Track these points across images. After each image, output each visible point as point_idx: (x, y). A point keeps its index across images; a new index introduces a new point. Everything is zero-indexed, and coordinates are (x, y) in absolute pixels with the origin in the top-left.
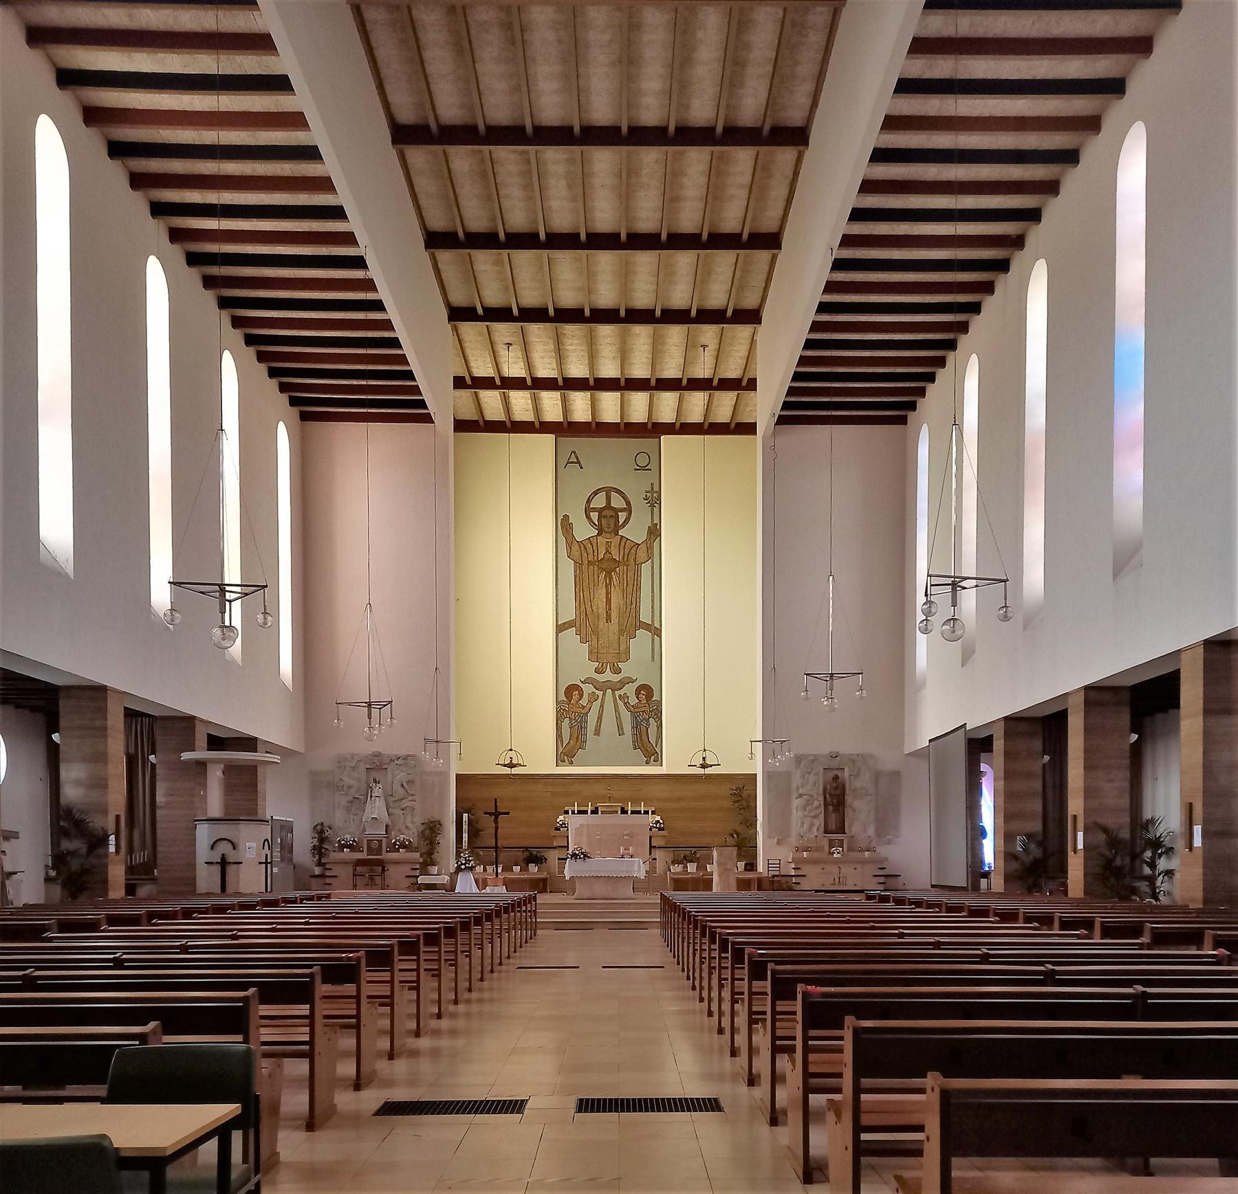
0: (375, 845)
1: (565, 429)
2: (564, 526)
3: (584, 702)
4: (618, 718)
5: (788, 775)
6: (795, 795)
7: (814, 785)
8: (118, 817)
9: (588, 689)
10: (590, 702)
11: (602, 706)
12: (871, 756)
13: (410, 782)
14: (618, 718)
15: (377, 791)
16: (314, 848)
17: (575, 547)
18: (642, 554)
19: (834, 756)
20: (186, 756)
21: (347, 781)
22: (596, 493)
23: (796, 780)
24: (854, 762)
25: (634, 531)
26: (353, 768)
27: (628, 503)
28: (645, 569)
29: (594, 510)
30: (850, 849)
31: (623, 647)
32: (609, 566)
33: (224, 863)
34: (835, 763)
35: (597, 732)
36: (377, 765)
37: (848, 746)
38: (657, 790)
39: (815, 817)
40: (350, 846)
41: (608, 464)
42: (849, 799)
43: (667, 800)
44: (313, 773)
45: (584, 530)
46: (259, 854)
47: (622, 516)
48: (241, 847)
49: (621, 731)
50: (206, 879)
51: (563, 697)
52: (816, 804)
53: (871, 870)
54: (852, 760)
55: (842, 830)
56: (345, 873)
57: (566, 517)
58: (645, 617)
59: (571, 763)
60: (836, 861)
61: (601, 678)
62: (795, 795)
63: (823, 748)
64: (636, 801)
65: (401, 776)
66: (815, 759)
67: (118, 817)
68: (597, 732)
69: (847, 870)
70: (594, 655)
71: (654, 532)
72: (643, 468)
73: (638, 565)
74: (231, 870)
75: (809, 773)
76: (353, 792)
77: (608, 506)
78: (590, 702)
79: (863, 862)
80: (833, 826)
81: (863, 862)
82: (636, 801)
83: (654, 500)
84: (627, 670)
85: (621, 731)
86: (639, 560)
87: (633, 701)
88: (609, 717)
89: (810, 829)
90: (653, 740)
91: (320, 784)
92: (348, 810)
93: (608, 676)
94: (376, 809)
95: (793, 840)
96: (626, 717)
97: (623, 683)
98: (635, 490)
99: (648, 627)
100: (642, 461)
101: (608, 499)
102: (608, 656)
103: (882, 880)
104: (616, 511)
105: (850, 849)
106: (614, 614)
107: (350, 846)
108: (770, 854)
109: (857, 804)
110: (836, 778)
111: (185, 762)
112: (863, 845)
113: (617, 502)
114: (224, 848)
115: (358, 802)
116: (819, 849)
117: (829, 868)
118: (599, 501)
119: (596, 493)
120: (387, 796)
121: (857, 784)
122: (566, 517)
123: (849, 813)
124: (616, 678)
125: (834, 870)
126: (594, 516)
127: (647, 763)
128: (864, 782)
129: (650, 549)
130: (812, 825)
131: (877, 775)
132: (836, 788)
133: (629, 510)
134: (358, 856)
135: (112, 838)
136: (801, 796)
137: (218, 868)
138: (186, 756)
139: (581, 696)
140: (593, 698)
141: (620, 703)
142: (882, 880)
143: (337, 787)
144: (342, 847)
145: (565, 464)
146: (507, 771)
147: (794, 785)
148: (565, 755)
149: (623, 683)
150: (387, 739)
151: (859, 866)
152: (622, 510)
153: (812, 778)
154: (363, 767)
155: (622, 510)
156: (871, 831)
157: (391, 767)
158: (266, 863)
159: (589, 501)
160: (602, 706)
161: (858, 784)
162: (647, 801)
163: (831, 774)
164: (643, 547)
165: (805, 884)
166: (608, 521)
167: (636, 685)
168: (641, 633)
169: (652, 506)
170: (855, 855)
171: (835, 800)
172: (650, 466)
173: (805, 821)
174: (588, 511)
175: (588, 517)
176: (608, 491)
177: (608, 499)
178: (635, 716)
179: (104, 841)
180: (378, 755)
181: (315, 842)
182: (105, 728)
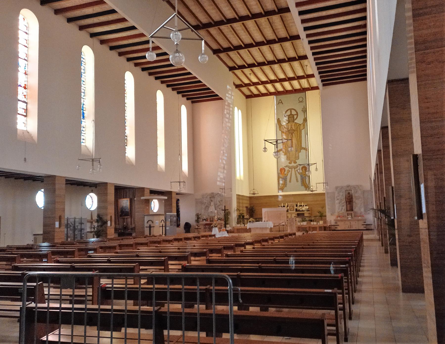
1: (277, 93)
2: (279, 121)
3: (286, 172)
4: (296, 177)
5: (334, 193)
6: (336, 199)
7: (342, 196)
8: (111, 217)
9: (287, 169)
11: (291, 174)
12: (361, 186)
13: (221, 201)
14: (296, 177)
15: (212, 204)
16: (196, 220)
18: (302, 127)
19: (348, 186)
20: (142, 198)
21: (205, 201)
22: (287, 111)
23: (336, 194)
24: (355, 188)
25: (299, 121)
26: (206, 197)
27: (297, 113)
28: (303, 132)
30: (355, 216)
31: (297, 155)
33: (150, 227)
34: (348, 189)
35: (290, 181)
36: (212, 196)
37: (353, 183)
38: (309, 199)
39: (343, 206)
40: (205, 220)
41: (291, 101)
42: (354, 200)
43: (312, 201)
44: (196, 199)
46: (159, 224)
47: (295, 117)
50: (147, 232)
51: (279, 172)
52: (343, 202)
53: (362, 223)
54: (354, 187)
55: (352, 210)
56: (202, 227)
58: (303, 146)
60: (349, 220)
61: (291, 165)
62: (336, 199)
63: (345, 184)
64: (301, 202)
65: (219, 199)
66: (342, 187)
67: (111, 217)
68: (290, 181)
69: (353, 223)
70: (288, 158)
71: (305, 120)
72: (301, 102)
74: (152, 228)
75: (340, 192)
76: (206, 204)
77: (291, 114)
79: (358, 220)
80: (348, 209)
81: (358, 220)
83: (305, 111)
84: (299, 162)
87: (301, 171)
89: (341, 210)
90: (307, 183)
91: (198, 202)
92: (205, 209)
93: (293, 164)
94: (212, 209)
95: (336, 214)
96: (299, 176)
97: (297, 166)
100: (301, 100)
101: (291, 112)
102: (292, 158)
103: (365, 226)
104: (293, 115)
106: (294, 146)
107: (205, 220)
108: (331, 219)
109: (357, 201)
110: (349, 193)
111: (143, 200)
113: (294, 113)
114: (150, 223)
115: (207, 207)
117: (347, 222)
118: (289, 113)
119: (287, 111)
120: (215, 205)
121: (355, 195)
123: (354, 204)
124: (295, 165)
125: (348, 223)
127: (306, 190)
129: (304, 125)
130: (342, 209)
131: (364, 192)
132: (349, 197)
134: (207, 222)
135: (109, 223)
136: (338, 199)
137: (148, 229)
138: (142, 198)
139: (285, 171)
141: (297, 172)
142: (365, 226)
143: (202, 203)
145: (279, 103)
146: (253, 195)
147: (336, 196)
148: (281, 189)
149: (297, 166)
151: (357, 222)
152: (295, 115)
153: (341, 194)
154: (209, 197)
155: (295, 115)
156: (362, 210)
157: (216, 196)
158: (163, 226)
160: (291, 174)
161: (357, 195)
162: (304, 202)
163: (347, 192)
164: (302, 125)
165: (339, 228)
166: (291, 118)
169: (304, 113)
170: (356, 218)
171: (349, 200)
172: (303, 101)
176: (291, 110)
177: (291, 112)
178: (301, 176)
179: (106, 223)
180: (213, 193)
181: (197, 219)
182: (107, 193)
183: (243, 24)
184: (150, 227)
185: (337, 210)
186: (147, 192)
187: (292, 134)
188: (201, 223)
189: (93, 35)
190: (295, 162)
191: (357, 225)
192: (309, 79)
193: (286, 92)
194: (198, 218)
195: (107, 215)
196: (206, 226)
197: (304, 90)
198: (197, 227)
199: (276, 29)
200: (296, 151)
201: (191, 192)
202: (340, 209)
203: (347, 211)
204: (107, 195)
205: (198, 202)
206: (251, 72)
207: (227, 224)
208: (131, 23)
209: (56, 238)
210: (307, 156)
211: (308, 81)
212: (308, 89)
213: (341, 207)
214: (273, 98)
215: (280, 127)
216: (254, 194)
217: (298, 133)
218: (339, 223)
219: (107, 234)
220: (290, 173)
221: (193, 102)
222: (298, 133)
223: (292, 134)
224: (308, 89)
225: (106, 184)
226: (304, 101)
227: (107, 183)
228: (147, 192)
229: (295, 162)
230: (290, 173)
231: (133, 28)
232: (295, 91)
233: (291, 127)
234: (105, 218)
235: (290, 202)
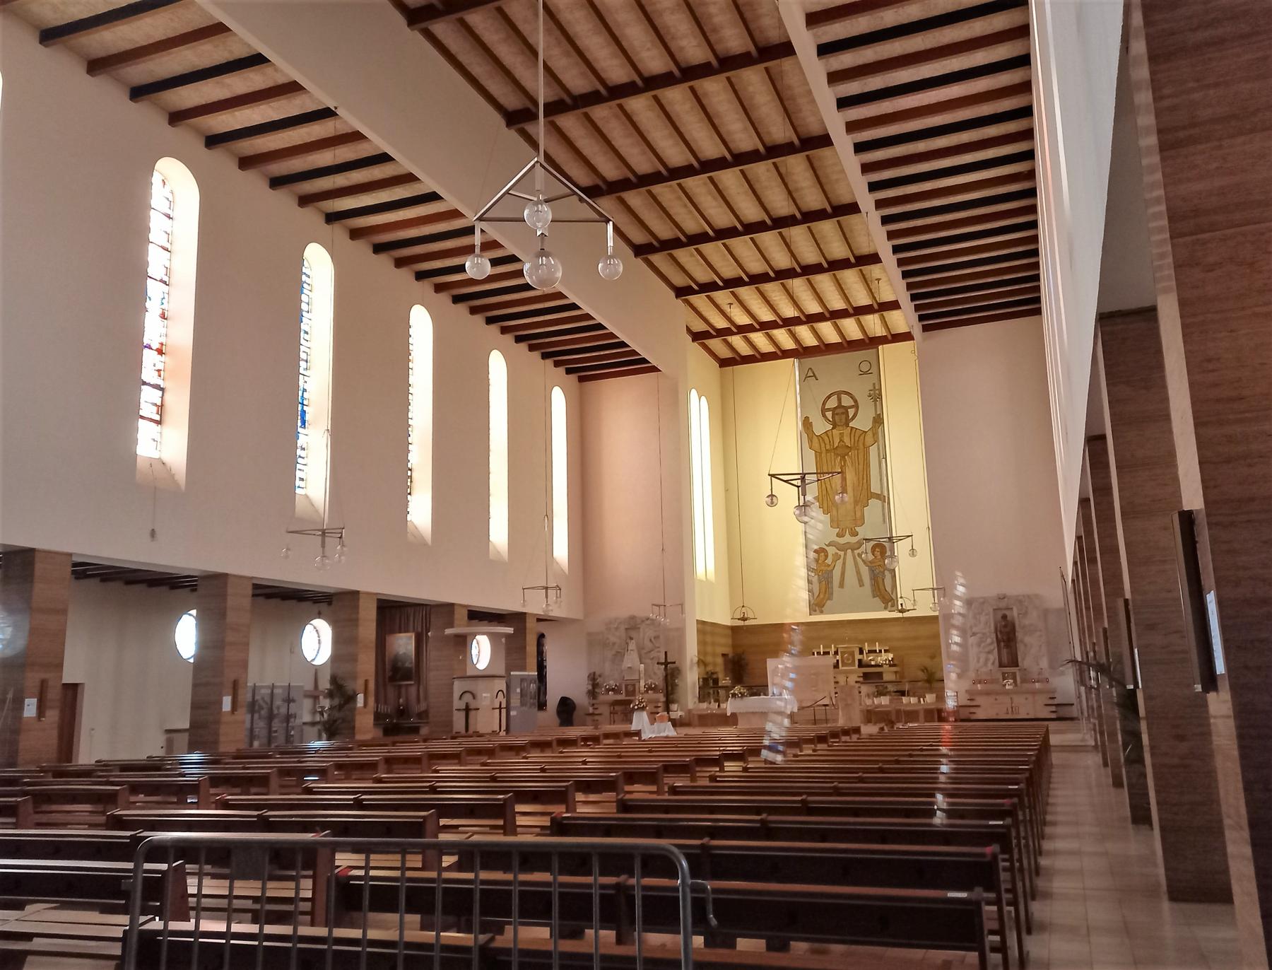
0: (630, 688)
1: (801, 352)
2: (807, 424)
3: (829, 561)
4: (858, 573)
7: (986, 625)
8: (366, 681)
9: (831, 551)
10: (835, 561)
11: (844, 563)
12: (1037, 596)
13: (657, 637)
14: (858, 573)
15: (632, 645)
16: (589, 692)
17: (815, 440)
18: (869, 438)
20: (448, 631)
21: (613, 639)
22: (829, 397)
24: (1020, 602)
25: (862, 422)
26: (617, 629)
27: (856, 401)
28: (873, 451)
29: (829, 410)
30: (1024, 681)
31: (858, 514)
32: (842, 453)
33: (467, 710)
34: (1003, 604)
35: (842, 585)
36: (633, 625)
37: (1015, 588)
38: (895, 632)
39: (989, 652)
40: (613, 690)
41: (839, 374)
42: (1019, 635)
44: (589, 634)
45: (821, 426)
46: (492, 702)
47: (851, 412)
48: (478, 696)
49: (861, 584)
50: (459, 723)
52: (989, 640)
53: (1042, 699)
54: (1020, 600)
55: (1015, 663)
56: (605, 710)
57: (807, 418)
58: (875, 488)
59: (822, 612)
60: (1007, 693)
61: (841, 541)
64: (872, 642)
65: (650, 633)
66: (984, 601)
67: (366, 681)
68: (842, 585)
69: (1019, 700)
70: (835, 523)
71: (878, 420)
72: (865, 373)
73: (866, 449)
74: (472, 714)
75: (980, 614)
77: (840, 406)
78: (835, 561)
79: (1034, 693)
80: (1005, 660)
82: (872, 642)
83: (876, 396)
84: (863, 532)
85: (861, 584)
86: (867, 444)
87: (871, 557)
88: (852, 571)
89: (986, 664)
90: (889, 589)
91: (595, 642)
93: (848, 538)
94: (631, 660)
95: (972, 675)
97: (859, 544)
98: (860, 389)
99: (880, 497)
100: (865, 367)
101: (839, 400)
102: (846, 523)
103: (1054, 709)
104: (846, 408)
105: (1024, 681)
106: (849, 489)
107: (613, 690)
109: (1027, 639)
110: (1004, 617)
111: (448, 636)
112: (1036, 677)
113: (846, 401)
114: (468, 697)
115: (619, 656)
116: (993, 681)
118: (832, 403)
119: (829, 397)
120: (640, 649)
121: (1026, 622)
122: (807, 418)
124: (854, 540)
125: (1007, 699)
126: (829, 415)
127: (886, 608)
128: (1033, 618)
129: (875, 434)
130: (987, 660)
131: (1046, 613)
132: (1005, 626)
133: (856, 406)
135: (360, 697)
136: (974, 634)
137: (463, 713)
138: (448, 631)
139: (826, 556)
140: (837, 557)
142: (1054, 709)
144: (608, 690)
145: (808, 376)
146: (741, 623)
148: (817, 605)
149: (859, 544)
150: (641, 608)
152: (851, 407)
153: (983, 619)
154: (623, 628)
155: (851, 407)
156: (1044, 663)
158: (500, 708)
159: (824, 404)
160: (844, 563)
161: (1026, 622)
163: (1000, 614)
164: (870, 434)
165: (981, 714)
166: (840, 416)
167: (873, 543)
168: (872, 502)
169: (875, 401)
170: (1027, 686)
171: (1007, 636)
172: (872, 371)
173: (985, 659)
174: (824, 411)
175: (824, 416)
176: (839, 394)
177: (839, 400)
178: (872, 571)
179: (351, 698)
180: (633, 618)
182: (357, 620)
183: (711, 179)
184: (467, 710)
185: (973, 664)
186: (461, 616)
187: (843, 457)
188: (602, 698)
189: (332, 218)
190: (855, 534)
191: (1029, 707)
192: (885, 313)
193: (825, 349)
194: (595, 685)
195: (354, 677)
196: (617, 708)
197: (872, 342)
198: (591, 710)
199: (797, 190)
200: (856, 502)
201: (579, 616)
202: (982, 660)
203: (1001, 665)
204: (357, 626)
205: (595, 642)
206: (733, 300)
207: (673, 702)
208: (318, 97)
209: (222, 739)
210: (886, 517)
211: (883, 319)
212: (883, 340)
213: (983, 657)
214: (791, 365)
215: (810, 440)
216: (744, 619)
217: (861, 456)
218: (980, 700)
219: (354, 728)
220: (839, 563)
221: (581, 379)
222: (861, 456)
223: (843, 457)
224: (883, 340)
225: (355, 594)
226: (874, 370)
227: (358, 592)
228: (461, 616)
229: (855, 534)
230: (839, 563)
231: (292, 88)
232: (849, 345)
233: (841, 440)
234: (350, 686)
235: (843, 642)
